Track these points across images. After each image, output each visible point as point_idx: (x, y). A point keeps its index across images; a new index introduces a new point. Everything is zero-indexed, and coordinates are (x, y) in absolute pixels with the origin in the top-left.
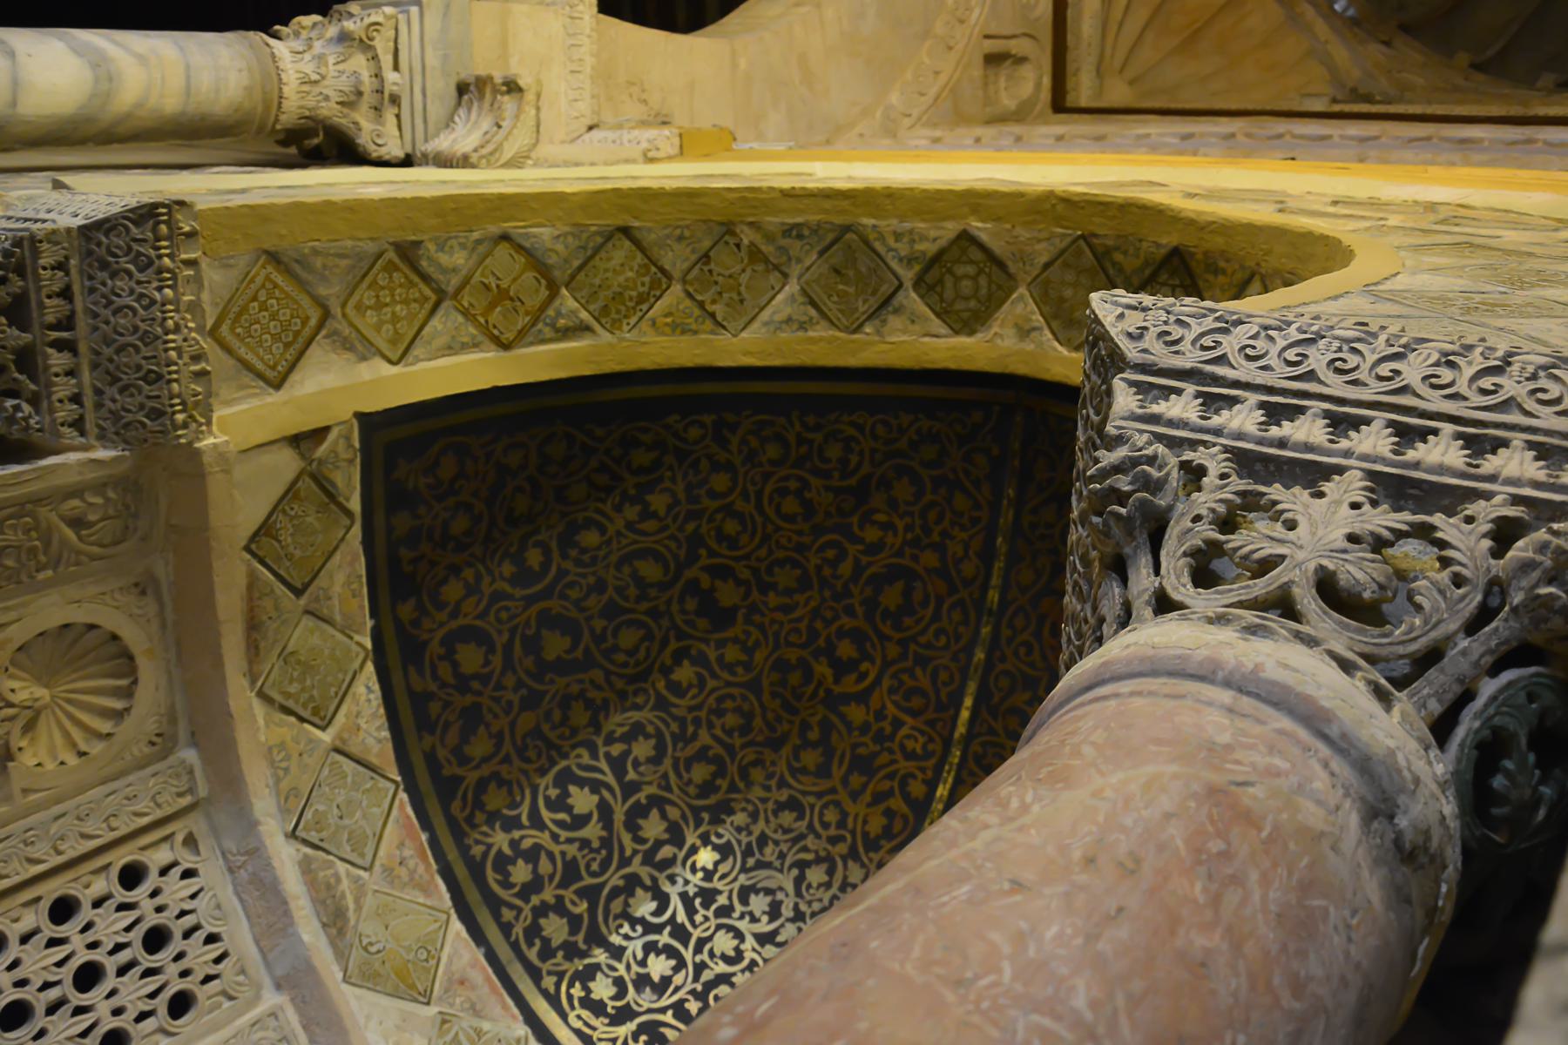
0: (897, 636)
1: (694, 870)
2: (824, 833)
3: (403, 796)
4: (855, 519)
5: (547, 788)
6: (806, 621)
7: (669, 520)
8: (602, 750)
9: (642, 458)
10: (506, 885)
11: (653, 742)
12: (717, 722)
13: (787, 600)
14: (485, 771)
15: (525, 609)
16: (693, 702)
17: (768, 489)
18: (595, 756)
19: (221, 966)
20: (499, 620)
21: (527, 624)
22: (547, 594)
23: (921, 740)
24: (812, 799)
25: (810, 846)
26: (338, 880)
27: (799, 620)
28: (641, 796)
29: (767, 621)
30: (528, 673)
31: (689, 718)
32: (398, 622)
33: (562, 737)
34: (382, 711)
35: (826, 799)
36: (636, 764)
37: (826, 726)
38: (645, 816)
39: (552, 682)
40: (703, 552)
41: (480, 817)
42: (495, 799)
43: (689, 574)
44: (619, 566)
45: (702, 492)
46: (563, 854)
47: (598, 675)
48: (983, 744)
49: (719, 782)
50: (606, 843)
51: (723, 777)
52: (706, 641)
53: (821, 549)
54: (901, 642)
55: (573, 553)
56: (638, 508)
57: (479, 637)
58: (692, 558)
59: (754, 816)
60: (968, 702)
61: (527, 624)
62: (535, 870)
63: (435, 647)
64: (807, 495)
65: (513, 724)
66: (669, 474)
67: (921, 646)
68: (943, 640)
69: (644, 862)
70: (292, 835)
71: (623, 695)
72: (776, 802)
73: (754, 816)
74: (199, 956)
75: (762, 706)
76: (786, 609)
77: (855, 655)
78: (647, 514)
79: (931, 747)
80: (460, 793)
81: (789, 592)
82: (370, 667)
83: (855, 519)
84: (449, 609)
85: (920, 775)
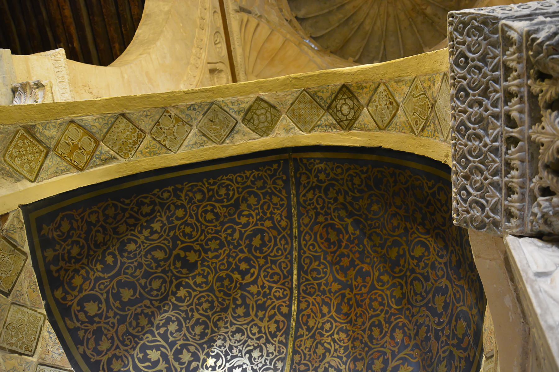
0: (262, 255)
2: (254, 337)
4: (236, 216)
5: (137, 355)
6: (225, 260)
7: (163, 233)
8: (156, 333)
9: (146, 209)
11: (176, 323)
13: (216, 253)
14: (110, 355)
15: (111, 282)
16: (188, 303)
17: (200, 211)
20: (100, 289)
22: (118, 274)
23: (281, 291)
24: (245, 326)
25: (250, 344)
27: (223, 259)
28: (177, 346)
29: (210, 263)
30: (117, 308)
31: (188, 309)
33: (138, 332)
34: (58, 341)
35: (250, 325)
36: (172, 334)
37: (243, 297)
38: (182, 353)
39: (129, 310)
40: (179, 242)
43: (175, 253)
44: (145, 256)
45: (174, 218)
47: (147, 302)
49: (207, 331)
51: (208, 329)
52: (187, 278)
54: (264, 258)
55: (126, 254)
56: (149, 230)
57: (95, 299)
58: (175, 246)
59: (224, 340)
60: (295, 272)
63: (75, 307)
64: (216, 211)
66: (159, 214)
67: (271, 256)
68: (280, 252)
71: (159, 308)
72: (232, 332)
73: (224, 340)
75: (217, 297)
76: (217, 257)
77: (248, 267)
78: (153, 232)
79: (285, 293)
80: (101, 368)
81: (216, 250)
82: (47, 323)
83: (236, 216)
84: (78, 289)
85: (284, 304)
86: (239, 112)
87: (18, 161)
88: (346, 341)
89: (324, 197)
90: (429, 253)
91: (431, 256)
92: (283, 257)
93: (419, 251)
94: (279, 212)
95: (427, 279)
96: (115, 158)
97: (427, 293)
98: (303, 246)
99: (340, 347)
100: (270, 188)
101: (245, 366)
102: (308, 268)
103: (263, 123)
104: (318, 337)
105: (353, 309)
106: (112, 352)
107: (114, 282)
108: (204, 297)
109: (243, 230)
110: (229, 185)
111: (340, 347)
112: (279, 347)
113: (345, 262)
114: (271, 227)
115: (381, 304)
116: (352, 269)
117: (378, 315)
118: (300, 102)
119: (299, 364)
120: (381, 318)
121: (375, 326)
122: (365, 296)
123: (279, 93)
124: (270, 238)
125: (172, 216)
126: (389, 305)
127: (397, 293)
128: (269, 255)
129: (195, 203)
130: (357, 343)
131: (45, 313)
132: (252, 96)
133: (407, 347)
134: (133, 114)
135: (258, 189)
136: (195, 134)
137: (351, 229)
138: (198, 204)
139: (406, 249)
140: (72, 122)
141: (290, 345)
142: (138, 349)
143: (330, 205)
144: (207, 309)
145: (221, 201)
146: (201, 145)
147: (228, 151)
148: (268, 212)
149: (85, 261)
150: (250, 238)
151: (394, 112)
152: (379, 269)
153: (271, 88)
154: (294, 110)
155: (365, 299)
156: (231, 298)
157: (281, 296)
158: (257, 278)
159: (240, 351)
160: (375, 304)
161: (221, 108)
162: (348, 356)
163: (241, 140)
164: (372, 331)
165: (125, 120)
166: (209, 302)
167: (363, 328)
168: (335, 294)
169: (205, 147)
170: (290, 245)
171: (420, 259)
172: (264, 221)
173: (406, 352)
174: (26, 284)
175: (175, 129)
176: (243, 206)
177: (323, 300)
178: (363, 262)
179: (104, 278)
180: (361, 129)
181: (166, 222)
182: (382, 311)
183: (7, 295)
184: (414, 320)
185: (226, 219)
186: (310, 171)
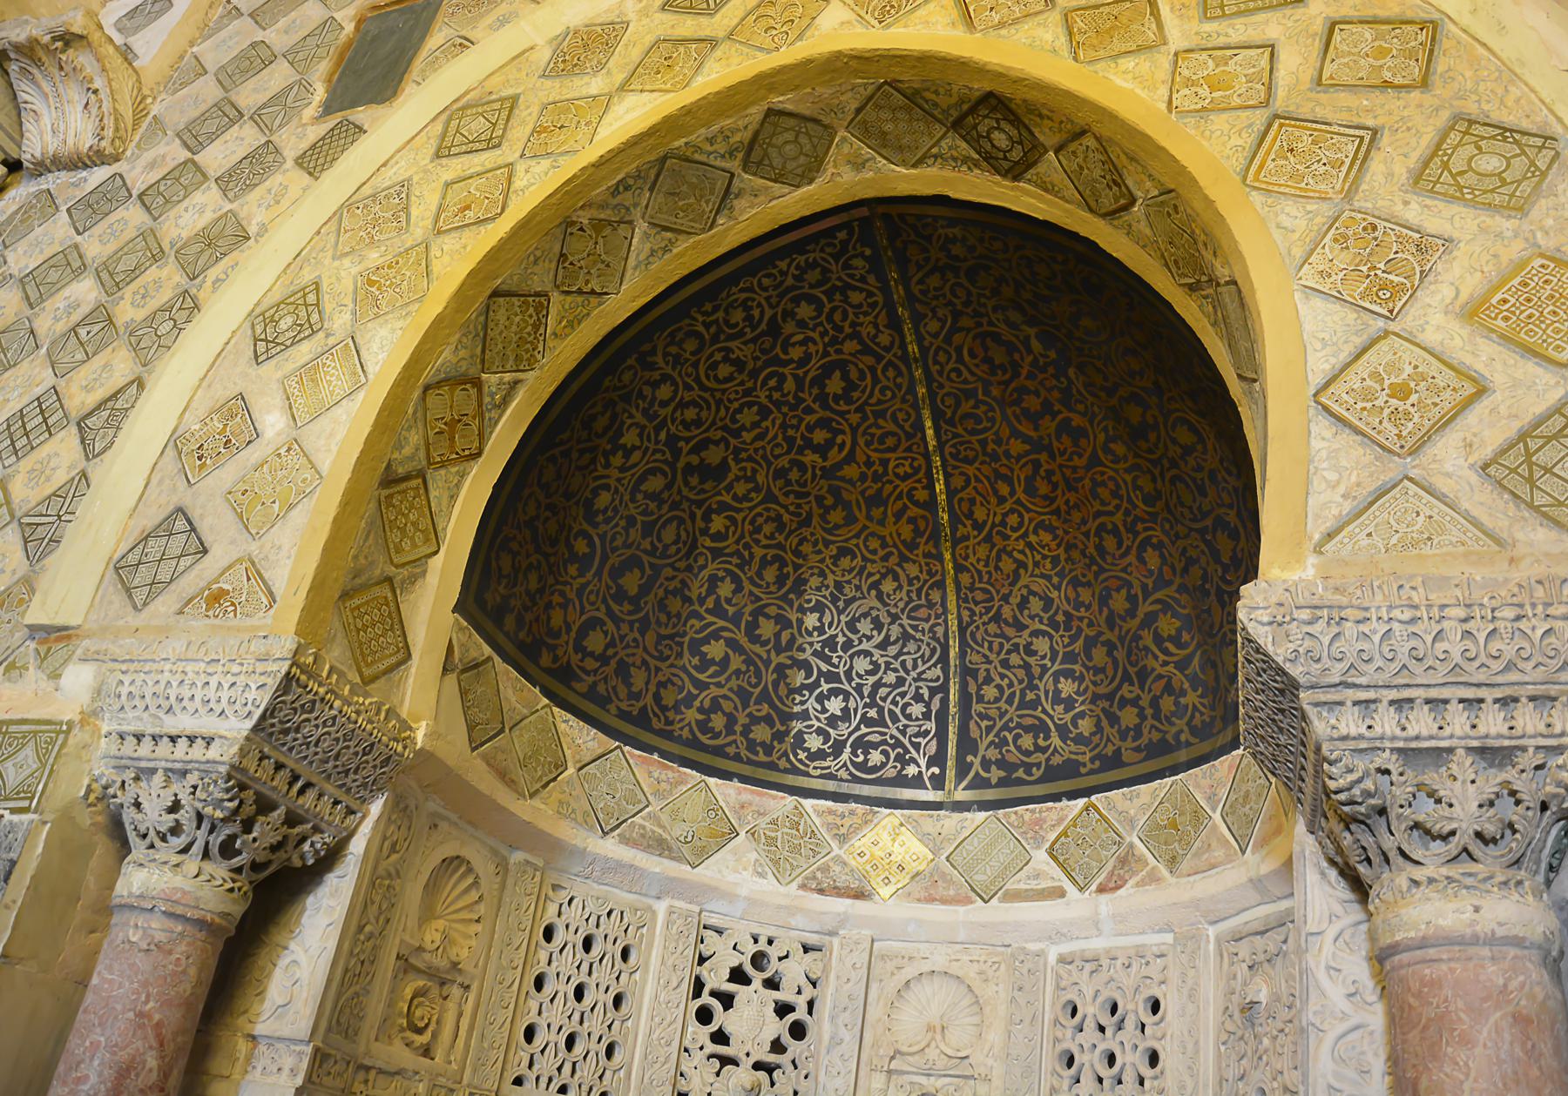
0: (853, 407)
1: (810, 634)
3: (627, 748)
4: (778, 349)
6: (780, 436)
7: (646, 443)
8: (702, 611)
9: (601, 423)
10: (717, 736)
12: (761, 537)
14: (652, 688)
19: (626, 920)
20: (593, 604)
21: (609, 588)
24: (854, 541)
26: (644, 828)
27: (775, 437)
30: (630, 613)
32: (548, 671)
33: (674, 626)
36: (728, 601)
37: (835, 492)
41: (671, 715)
42: (669, 698)
43: (680, 465)
44: (633, 500)
46: (731, 689)
47: (668, 572)
48: (953, 446)
50: (749, 662)
53: (764, 383)
54: (856, 411)
55: (600, 518)
56: (620, 453)
57: (593, 623)
58: (677, 453)
59: (822, 574)
60: (928, 423)
61: (609, 588)
62: (724, 713)
63: (575, 659)
64: (733, 356)
68: (889, 394)
70: (605, 833)
71: (689, 568)
74: (611, 927)
75: (785, 507)
76: (760, 437)
77: (829, 436)
78: (628, 453)
79: (916, 464)
81: (755, 425)
82: (556, 710)
83: (778, 349)
87: (406, 544)
88: (1053, 545)
89: (966, 284)
90: (1205, 452)
92: (898, 400)
93: (1184, 436)
94: (869, 318)
96: (516, 383)
97: (1205, 515)
98: (936, 376)
99: (1045, 557)
100: (840, 279)
101: (874, 613)
102: (954, 413)
104: (997, 539)
105: (1059, 491)
106: (654, 681)
107: (605, 575)
108: (761, 515)
109: (800, 372)
110: (747, 299)
111: (1045, 557)
112: (927, 564)
113: (1033, 403)
115: (1115, 494)
116: (1048, 417)
118: (879, 107)
119: (972, 589)
120: (1118, 518)
121: (1108, 532)
122: (1081, 472)
123: (819, 90)
124: (861, 371)
125: (652, 404)
126: (1130, 500)
128: (866, 403)
129: (687, 360)
130: (1076, 555)
131: (546, 701)
133: (1168, 583)
134: (511, 276)
135: (812, 286)
136: (646, 235)
137: (1036, 345)
138: (694, 359)
139: (1160, 420)
140: (427, 388)
141: (948, 556)
143: (983, 300)
144: (772, 534)
145: (742, 334)
146: (666, 250)
147: (729, 239)
149: (551, 580)
150: (819, 381)
151: (1122, 201)
153: (797, 82)
155: (1082, 479)
156: (811, 498)
157: (909, 471)
158: (852, 451)
159: (858, 588)
160: (1104, 493)
161: (688, 160)
162: (1061, 575)
163: (752, 207)
164: (1101, 539)
165: (501, 300)
166: (773, 520)
167: (1084, 529)
168: (1018, 459)
169: (675, 251)
170: (907, 377)
171: (1187, 450)
174: (510, 691)
176: (789, 327)
177: (995, 470)
178: (1070, 410)
179: (589, 582)
180: (1046, 190)
181: (644, 421)
182: (1118, 507)
183: (502, 731)
184: (1180, 543)
185: (759, 363)
186: (929, 238)
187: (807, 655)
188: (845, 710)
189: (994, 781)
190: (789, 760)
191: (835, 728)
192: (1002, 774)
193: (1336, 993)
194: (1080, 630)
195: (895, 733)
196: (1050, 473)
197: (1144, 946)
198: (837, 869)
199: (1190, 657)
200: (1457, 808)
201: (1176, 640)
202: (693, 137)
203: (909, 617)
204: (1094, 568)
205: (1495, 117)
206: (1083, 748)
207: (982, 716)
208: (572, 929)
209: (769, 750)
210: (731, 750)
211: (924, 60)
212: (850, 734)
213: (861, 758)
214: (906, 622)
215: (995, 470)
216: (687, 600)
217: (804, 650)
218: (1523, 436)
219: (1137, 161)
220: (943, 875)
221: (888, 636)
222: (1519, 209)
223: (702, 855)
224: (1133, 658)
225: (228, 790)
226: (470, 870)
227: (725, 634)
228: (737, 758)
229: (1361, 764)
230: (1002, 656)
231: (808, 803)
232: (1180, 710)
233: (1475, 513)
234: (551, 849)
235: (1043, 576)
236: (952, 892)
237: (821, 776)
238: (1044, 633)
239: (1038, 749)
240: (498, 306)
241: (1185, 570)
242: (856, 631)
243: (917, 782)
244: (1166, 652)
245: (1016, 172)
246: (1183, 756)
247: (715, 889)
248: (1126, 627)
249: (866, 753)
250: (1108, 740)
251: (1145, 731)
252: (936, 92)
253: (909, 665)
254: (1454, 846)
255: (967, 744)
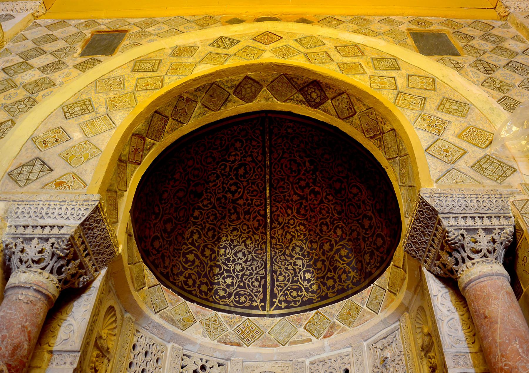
1: (221, 256)
3: (162, 285)
8: (188, 243)
10: (190, 287)
14: (171, 267)
18: (187, 246)
20: (157, 231)
22: (162, 216)
24: (239, 226)
27: (219, 186)
28: (201, 248)
30: (167, 238)
33: (179, 246)
36: (196, 241)
38: (205, 251)
42: (176, 271)
48: (275, 197)
50: (201, 263)
53: (220, 167)
55: (163, 202)
57: (156, 238)
59: (227, 236)
60: (268, 188)
65: (170, 252)
68: (257, 177)
69: (211, 262)
70: (156, 313)
71: (185, 227)
73: (227, 236)
75: (218, 211)
76: (215, 185)
81: (214, 181)
86: (231, 88)
90: (362, 194)
91: (363, 196)
93: (355, 191)
95: (359, 207)
96: (154, 144)
97: (359, 215)
99: (301, 234)
101: (243, 251)
103: (249, 93)
104: (286, 228)
105: (308, 212)
106: (171, 264)
107: (162, 222)
108: (210, 212)
111: (301, 234)
113: (303, 183)
114: (251, 161)
115: (327, 212)
117: (326, 219)
119: (276, 244)
121: (324, 225)
122: (316, 206)
124: (250, 168)
126: (332, 214)
127: (338, 208)
128: (250, 179)
130: (312, 233)
132: (241, 75)
134: (162, 107)
137: (307, 164)
141: (268, 233)
142: (181, 257)
146: (204, 114)
148: (249, 151)
150: (237, 169)
151: (351, 114)
152: (326, 192)
153: (257, 69)
154: (273, 86)
155: (316, 208)
159: (238, 242)
160: (324, 212)
161: (219, 86)
162: (306, 240)
164: (321, 227)
167: (315, 224)
172: (246, 157)
173: (344, 241)
175: (186, 108)
178: (315, 185)
180: (325, 112)
182: (328, 216)
184: (349, 225)
187: (220, 263)
188: (232, 283)
189: (283, 307)
190: (213, 298)
191: (229, 288)
192: (286, 305)
193: (444, 310)
194: (312, 257)
195: (249, 291)
196: (305, 206)
197: (341, 353)
198: (231, 336)
199: (351, 261)
200: (482, 243)
201: (347, 256)
202: (222, 79)
203: (254, 253)
204: (318, 236)
205: (453, 98)
206: (314, 295)
207: (278, 286)
208: (142, 347)
209: (206, 294)
210: (194, 293)
211: (297, 68)
212: (234, 291)
213: (237, 299)
214: (253, 254)
215: (287, 206)
216: (183, 238)
217: (219, 261)
218: (478, 162)
219: (360, 101)
220: (268, 338)
221: (247, 259)
222: (465, 117)
223: (185, 327)
224: (332, 264)
225: (67, 245)
226: (115, 315)
227: (194, 252)
228: (196, 295)
229: (457, 233)
230: (286, 266)
231: (220, 314)
232: (348, 278)
233: (472, 176)
234: (138, 313)
235: (300, 240)
236: (271, 343)
237: (224, 305)
238: (300, 259)
239: (298, 296)
240: (156, 118)
241: (351, 234)
242: (237, 256)
243: (257, 308)
244: (344, 260)
245: (316, 106)
246: (350, 292)
247: (189, 340)
248: (329, 254)
249: (239, 298)
250: (323, 291)
251: (336, 286)
252: (298, 79)
253: (254, 269)
254: (481, 254)
255: (273, 296)
